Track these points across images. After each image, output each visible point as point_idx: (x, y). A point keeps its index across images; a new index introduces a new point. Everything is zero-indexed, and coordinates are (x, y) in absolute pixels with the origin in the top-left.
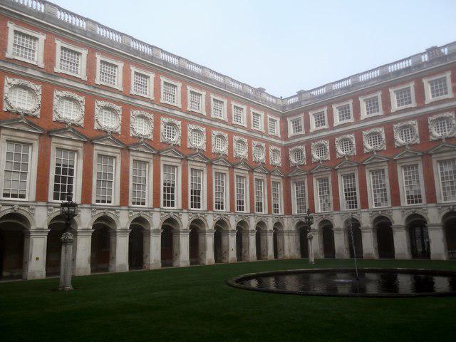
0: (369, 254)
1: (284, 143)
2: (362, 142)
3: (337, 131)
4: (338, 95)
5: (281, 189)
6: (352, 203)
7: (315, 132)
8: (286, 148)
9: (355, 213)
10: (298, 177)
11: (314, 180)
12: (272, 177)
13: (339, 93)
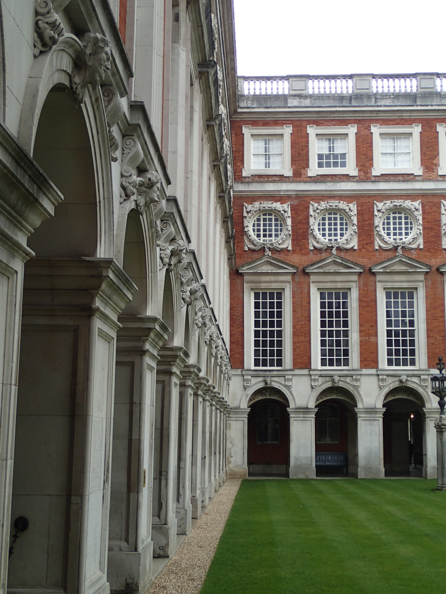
0: (368, 469)
3: (382, 186)
4: (385, 105)
6: (335, 352)
10: (264, 278)
13: (388, 102)
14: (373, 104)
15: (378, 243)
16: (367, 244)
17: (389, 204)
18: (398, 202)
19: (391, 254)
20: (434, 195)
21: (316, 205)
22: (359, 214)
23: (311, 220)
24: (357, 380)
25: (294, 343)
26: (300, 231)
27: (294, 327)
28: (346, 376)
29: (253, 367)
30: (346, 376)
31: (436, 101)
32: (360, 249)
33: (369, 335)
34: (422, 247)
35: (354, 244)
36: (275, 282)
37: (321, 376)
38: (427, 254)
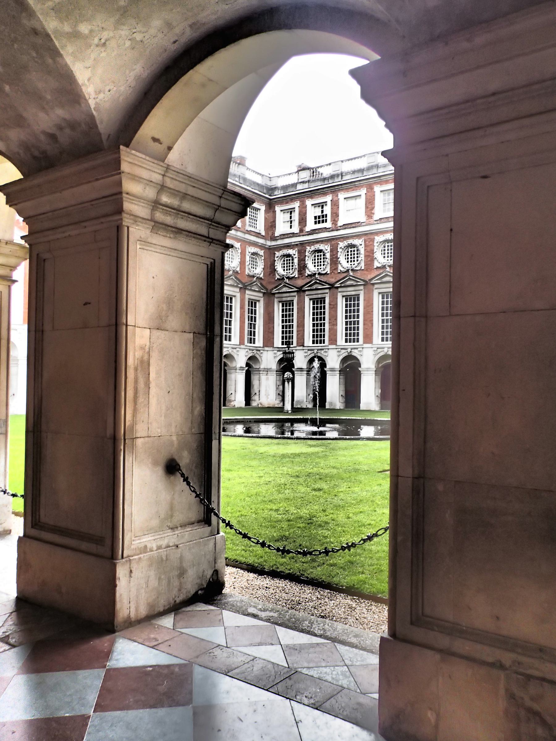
1: (269, 243)
2: (372, 252)
4: (348, 178)
5: (260, 308)
7: (313, 232)
8: (271, 251)
9: (355, 349)
11: (307, 299)
12: (247, 292)
14: (340, 180)
15: (340, 268)
16: (334, 269)
17: (346, 243)
18: (350, 241)
19: (345, 274)
20: (371, 233)
21: (308, 248)
22: (331, 251)
23: (307, 258)
24: (326, 352)
25: (297, 331)
26: (302, 265)
27: (298, 322)
28: (321, 350)
29: (280, 346)
30: (321, 350)
31: (375, 171)
32: (331, 273)
33: (334, 325)
34: (363, 268)
35: (328, 270)
36: (289, 297)
37: (308, 350)
38: (366, 272)
